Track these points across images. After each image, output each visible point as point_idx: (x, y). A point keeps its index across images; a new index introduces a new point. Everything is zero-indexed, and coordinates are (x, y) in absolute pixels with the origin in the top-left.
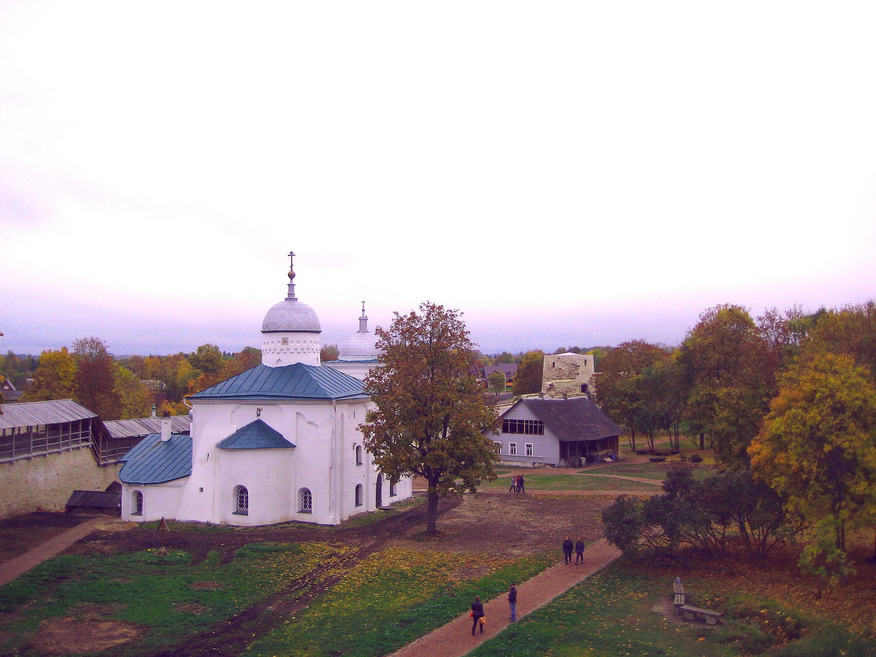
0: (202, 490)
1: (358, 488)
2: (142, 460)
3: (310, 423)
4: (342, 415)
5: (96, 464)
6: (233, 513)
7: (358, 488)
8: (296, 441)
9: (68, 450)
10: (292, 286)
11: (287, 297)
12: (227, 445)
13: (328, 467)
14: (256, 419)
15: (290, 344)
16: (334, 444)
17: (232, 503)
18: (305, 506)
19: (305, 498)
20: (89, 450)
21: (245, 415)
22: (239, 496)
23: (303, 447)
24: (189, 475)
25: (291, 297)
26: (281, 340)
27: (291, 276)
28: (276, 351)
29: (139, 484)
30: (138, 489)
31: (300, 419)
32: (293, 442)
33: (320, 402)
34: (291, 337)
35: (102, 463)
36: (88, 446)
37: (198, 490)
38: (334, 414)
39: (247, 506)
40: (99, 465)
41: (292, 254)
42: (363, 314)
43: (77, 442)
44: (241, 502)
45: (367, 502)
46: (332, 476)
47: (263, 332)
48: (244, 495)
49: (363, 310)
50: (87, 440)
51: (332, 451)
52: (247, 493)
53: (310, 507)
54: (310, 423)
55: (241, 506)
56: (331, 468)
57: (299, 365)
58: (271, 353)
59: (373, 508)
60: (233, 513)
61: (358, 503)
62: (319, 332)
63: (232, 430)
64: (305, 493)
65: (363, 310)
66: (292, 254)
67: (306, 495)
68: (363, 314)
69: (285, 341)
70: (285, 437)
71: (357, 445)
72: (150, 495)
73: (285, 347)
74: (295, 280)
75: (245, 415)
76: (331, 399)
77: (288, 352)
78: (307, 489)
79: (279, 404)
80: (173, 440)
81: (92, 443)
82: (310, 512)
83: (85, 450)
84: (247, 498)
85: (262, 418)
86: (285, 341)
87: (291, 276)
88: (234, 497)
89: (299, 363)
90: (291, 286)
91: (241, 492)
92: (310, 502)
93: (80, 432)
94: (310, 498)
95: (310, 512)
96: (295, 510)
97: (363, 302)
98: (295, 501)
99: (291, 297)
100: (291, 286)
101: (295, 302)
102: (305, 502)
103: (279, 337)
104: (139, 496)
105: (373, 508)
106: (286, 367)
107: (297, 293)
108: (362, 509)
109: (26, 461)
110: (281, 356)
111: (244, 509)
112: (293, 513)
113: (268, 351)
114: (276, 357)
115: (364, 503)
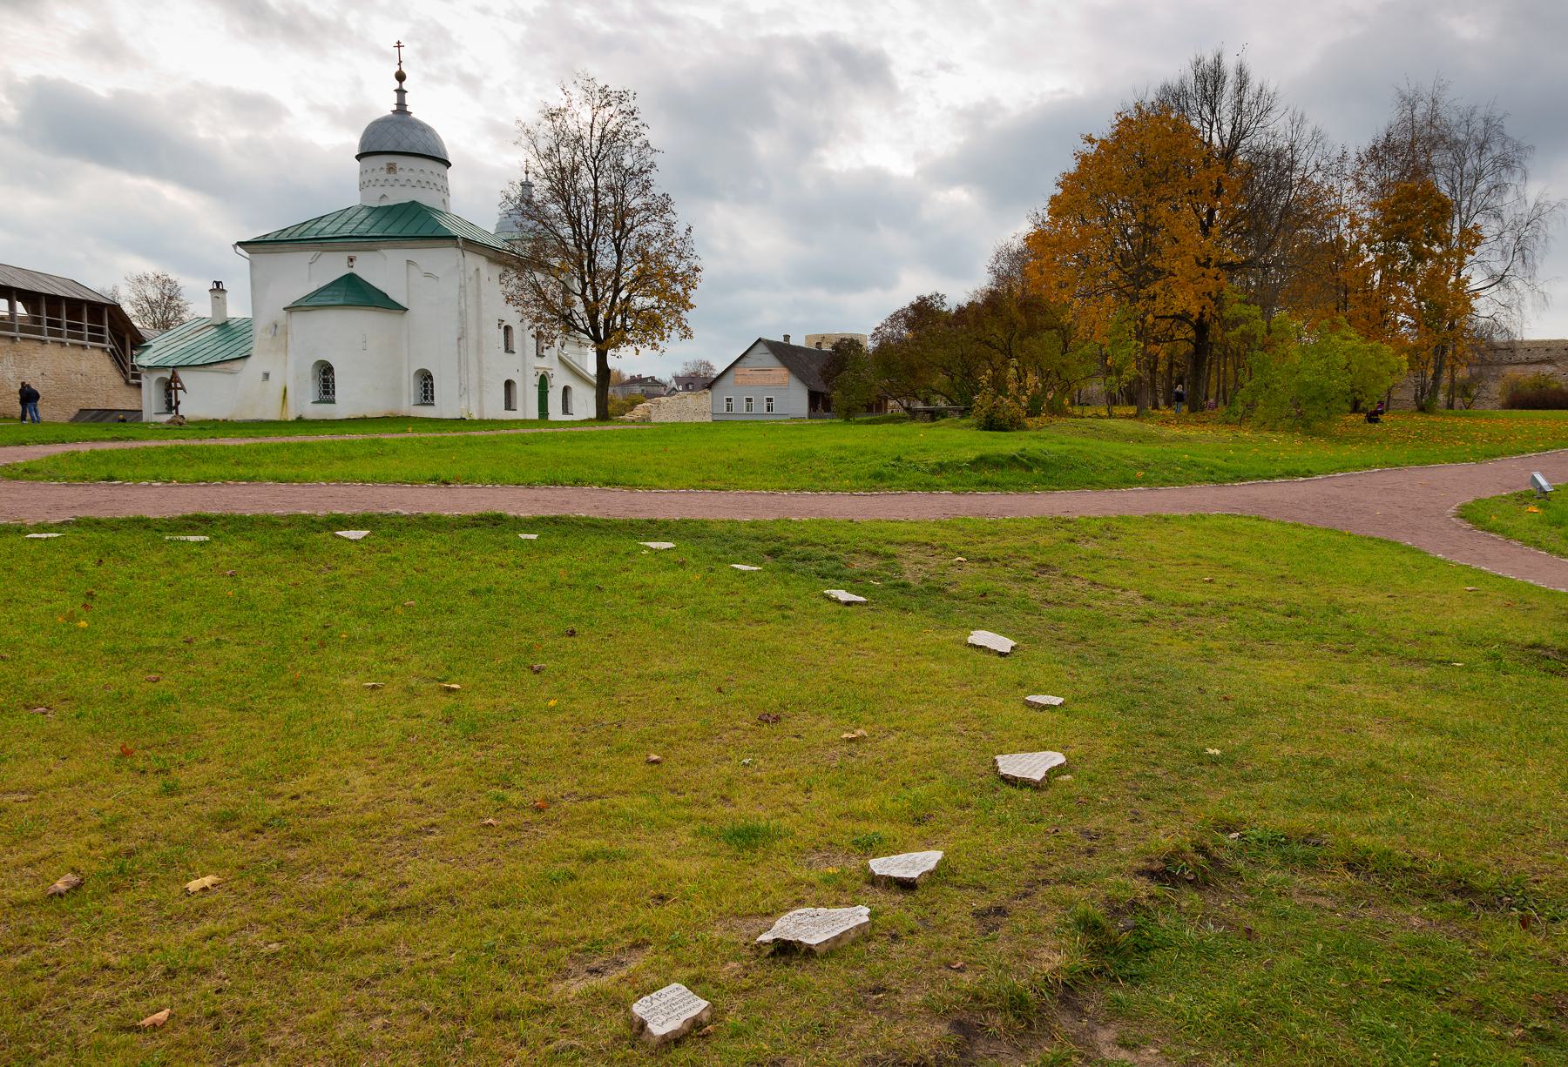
0: (267, 376)
3: (428, 275)
4: (478, 270)
7: (509, 385)
8: (408, 302)
11: (395, 108)
13: (456, 337)
14: (348, 271)
16: (463, 305)
17: (311, 389)
18: (426, 398)
19: (426, 386)
20: (107, 357)
21: (332, 267)
22: (324, 380)
23: (419, 311)
24: (248, 356)
25: (401, 107)
26: (385, 167)
27: (401, 77)
28: (378, 184)
31: (412, 268)
34: (400, 162)
36: (103, 349)
37: (261, 377)
38: (461, 262)
39: (334, 392)
40: (127, 383)
41: (399, 45)
44: (326, 386)
46: (462, 350)
50: (101, 340)
51: (460, 314)
53: (432, 398)
54: (428, 275)
55: (326, 393)
56: (459, 339)
57: (414, 202)
58: (371, 187)
61: (509, 405)
63: (313, 287)
64: (425, 379)
67: (426, 380)
71: (505, 324)
73: (391, 177)
74: (405, 85)
75: (332, 267)
76: (455, 238)
77: (397, 184)
79: (379, 249)
81: (112, 346)
83: (97, 353)
84: (333, 379)
85: (355, 271)
86: (391, 168)
87: (401, 77)
88: (314, 378)
90: (401, 92)
91: (325, 373)
92: (432, 392)
93: (86, 323)
94: (432, 385)
96: (409, 402)
99: (401, 107)
100: (401, 92)
102: (426, 392)
103: (384, 161)
106: (395, 206)
110: (387, 191)
112: (407, 405)
114: (379, 191)
115: (519, 407)
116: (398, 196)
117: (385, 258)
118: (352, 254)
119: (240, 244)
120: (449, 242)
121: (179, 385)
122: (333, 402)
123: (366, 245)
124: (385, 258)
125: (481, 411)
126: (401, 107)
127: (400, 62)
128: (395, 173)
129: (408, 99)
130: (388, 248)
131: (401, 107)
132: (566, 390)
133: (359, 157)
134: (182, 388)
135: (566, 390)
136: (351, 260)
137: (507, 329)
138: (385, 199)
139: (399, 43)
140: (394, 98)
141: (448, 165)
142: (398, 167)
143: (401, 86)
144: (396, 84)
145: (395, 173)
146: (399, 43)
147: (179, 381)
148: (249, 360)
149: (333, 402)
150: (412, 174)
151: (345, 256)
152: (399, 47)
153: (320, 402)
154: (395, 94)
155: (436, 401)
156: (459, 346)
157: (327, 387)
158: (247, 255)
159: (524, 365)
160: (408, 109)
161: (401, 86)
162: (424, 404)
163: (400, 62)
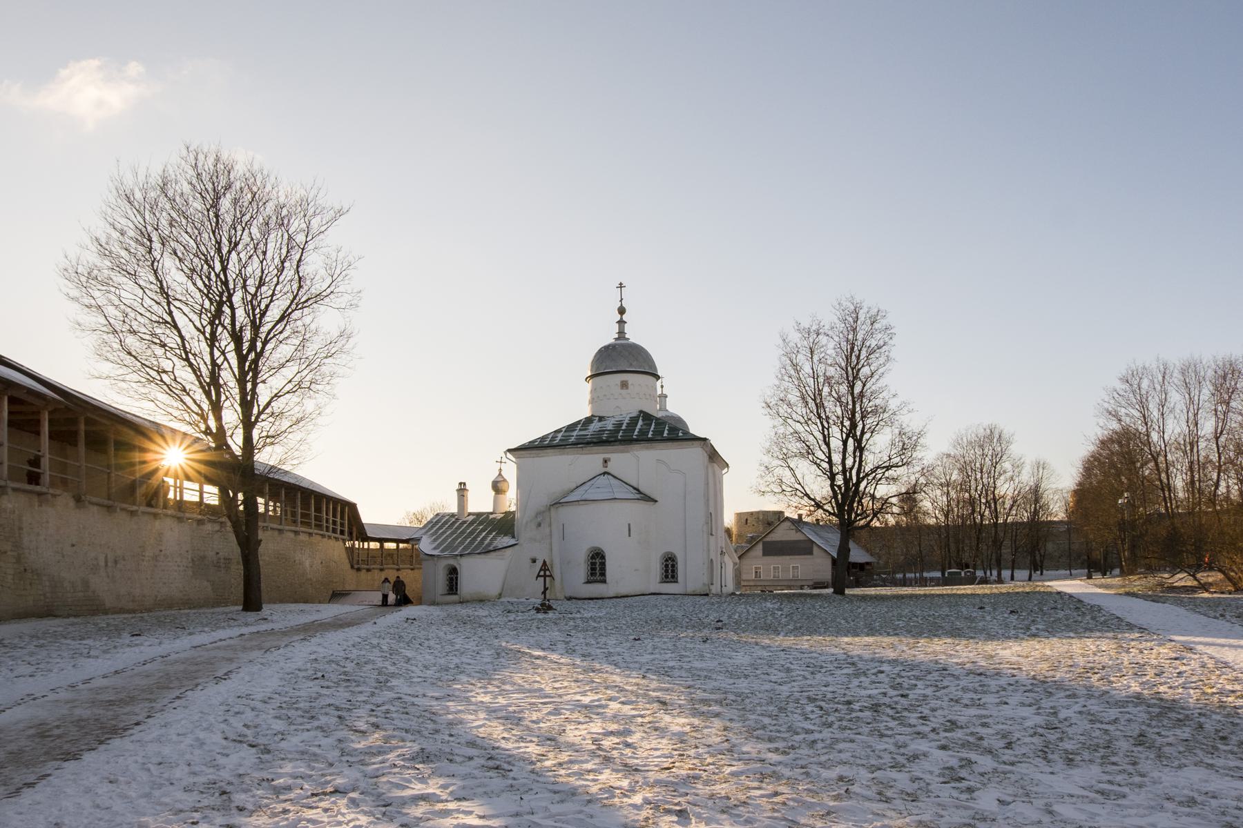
5: (349, 566)
9: (330, 537)
10: (622, 324)
11: (617, 336)
18: (667, 577)
19: (667, 566)
35: (356, 566)
40: (352, 567)
43: (334, 531)
48: (597, 561)
52: (603, 557)
53: (673, 577)
55: (592, 574)
64: (667, 560)
73: (624, 392)
74: (625, 318)
86: (624, 385)
92: (673, 571)
94: (673, 566)
95: (677, 582)
98: (656, 569)
102: (666, 571)
109: (292, 535)
118: (607, 456)
119: (509, 450)
121: (548, 573)
122: (604, 582)
128: (627, 388)
129: (627, 328)
134: (551, 576)
136: (606, 462)
140: (616, 328)
141: (657, 377)
142: (630, 383)
143: (621, 318)
145: (627, 388)
151: (601, 457)
154: (617, 325)
155: (680, 578)
158: (514, 459)
160: (627, 336)
161: (621, 318)
162: (665, 582)
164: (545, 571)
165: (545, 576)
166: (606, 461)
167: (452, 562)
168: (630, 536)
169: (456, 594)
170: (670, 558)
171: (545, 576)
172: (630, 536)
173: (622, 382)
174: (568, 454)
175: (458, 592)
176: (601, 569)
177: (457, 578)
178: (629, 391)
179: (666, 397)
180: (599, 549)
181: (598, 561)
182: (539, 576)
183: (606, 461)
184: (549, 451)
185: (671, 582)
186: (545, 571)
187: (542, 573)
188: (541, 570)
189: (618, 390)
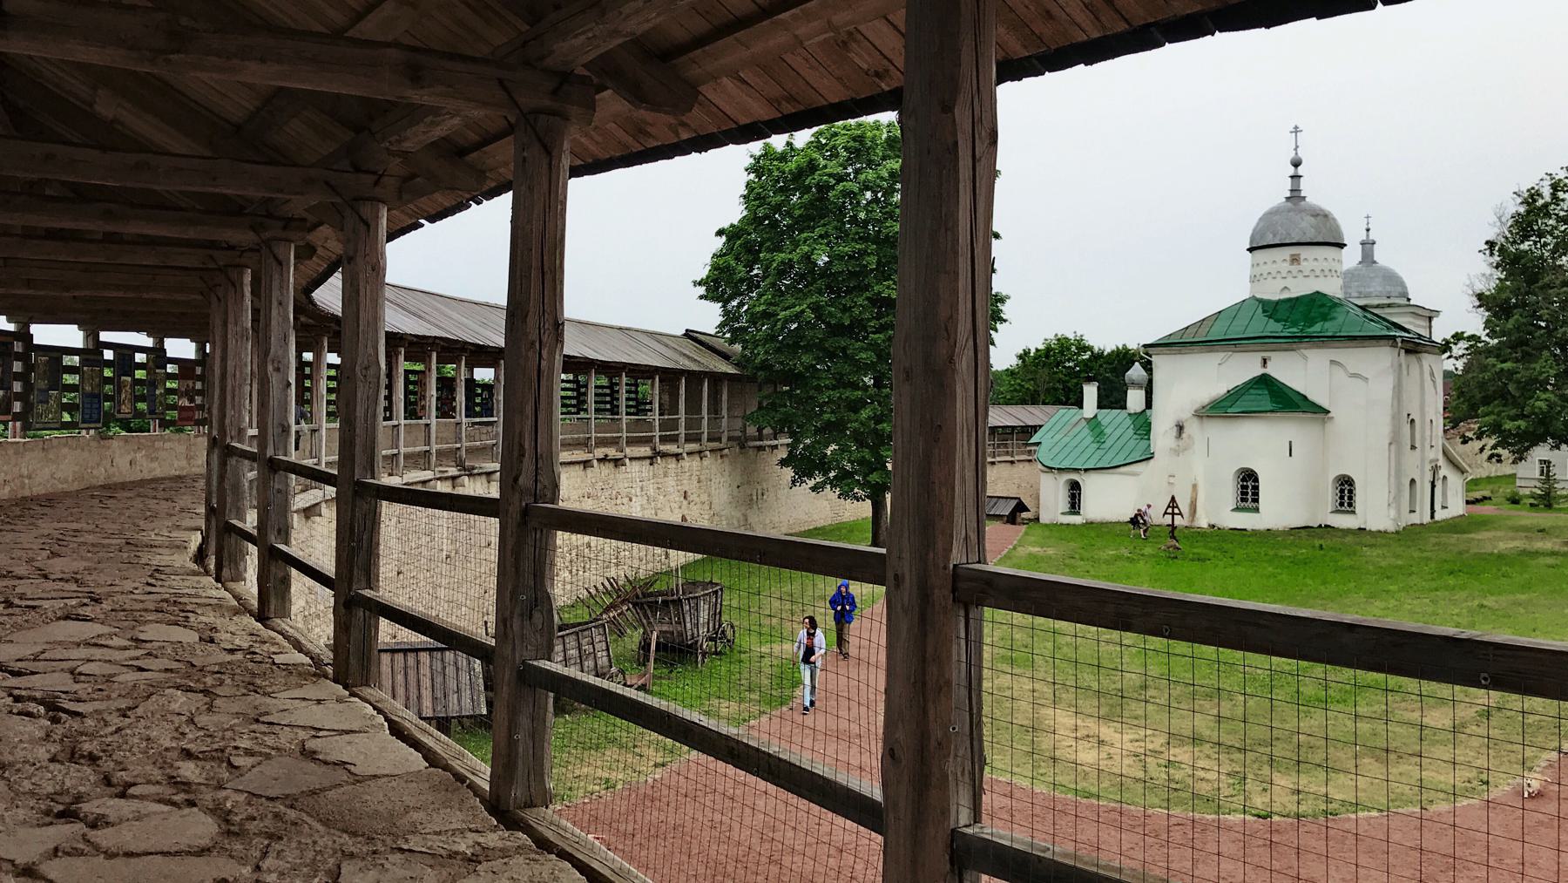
1: (1413, 481)
2: (1067, 439)
6: (1233, 510)
7: (1413, 481)
10: (1295, 179)
11: (1288, 195)
12: (1224, 408)
13: (1387, 442)
15: (1304, 264)
18: (1342, 504)
19: (1342, 491)
21: (1241, 369)
22: (1242, 487)
25: (1295, 196)
26: (1288, 258)
29: (1076, 470)
30: (1075, 477)
31: (1335, 368)
32: (1326, 406)
33: (1374, 342)
34: (1305, 252)
39: (1256, 500)
41: (1296, 130)
42: (1368, 236)
44: (1244, 493)
45: (1422, 509)
47: (1251, 250)
49: (1368, 230)
51: (1393, 418)
52: (1256, 480)
53: (1350, 505)
55: (1242, 500)
56: (1390, 444)
59: (1427, 519)
60: (1233, 510)
62: (1341, 246)
63: (1220, 388)
64: (1342, 484)
65: (1368, 230)
66: (1296, 130)
67: (1345, 489)
68: (1368, 236)
69: (1295, 260)
70: (1310, 397)
72: (1092, 486)
73: (1294, 268)
74: (1300, 170)
75: (1243, 368)
78: (1349, 477)
79: (1299, 349)
80: (1099, 418)
82: (1353, 512)
84: (1256, 488)
86: (1295, 260)
89: (1318, 292)
92: (1350, 498)
94: (1350, 492)
95: (1353, 512)
97: (1368, 217)
98: (1330, 495)
99: (1295, 196)
101: (1303, 203)
102: (1342, 498)
104: (1075, 487)
105: (1427, 519)
107: (1306, 187)
108: (1415, 519)
110: (1289, 282)
111: (1249, 504)
113: (1265, 275)
114: (1283, 283)
116: (1300, 288)
117: (1305, 358)
118: (1266, 354)
120: (1385, 342)
121: (1176, 511)
122: (1257, 510)
123: (1285, 346)
124: (1305, 358)
125: (1421, 519)
126: (1296, 194)
127: (1297, 147)
130: (1310, 348)
131: (1296, 194)
132: (1445, 477)
133: (1251, 250)
134: (1180, 514)
135: (1445, 477)
137: (1412, 421)
138: (1286, 291)
139: (1296, 127)
140: (1288, 184)
141: (1341, 246)
142: (1302, 257)
144: (1291, 170)
146: (1296, 127)
147: (1177, 507)
148: (1152, 461)
149: (1257, 510)
150: (1315, 263)
151: (1258, 357)
152: (1296, 132)
153: (1237, 509)
156: (1389, 450)
157: (1247, 493)
159: (1423, 460)
160: (1302, 195)
163: (1297, 147)
164: (1173, 508)
165: (1173, 514)
166: (1265, 361)
167: (1075, 477)
168: (1290, 455)
169: (1078, 513)
170: (1346, 482)
171: (1173, 514)
172: (1290, 455)
173: (1292, 255)
174: (1217, 351)
175: (1082, 511)
176: (1253, 494)
177: (1080, 494)
178: (1300, 267)
179: (1374, 243)
180: (1252, 471)
181: (1250, 484)
182: (1166, 513)
183: (1265, 361)
184: (1196, 348)
185: (1348, 512)
186: (1173, 508)
187: (1170, 510)
188: (1169, 506)
189: (1286, 266)
